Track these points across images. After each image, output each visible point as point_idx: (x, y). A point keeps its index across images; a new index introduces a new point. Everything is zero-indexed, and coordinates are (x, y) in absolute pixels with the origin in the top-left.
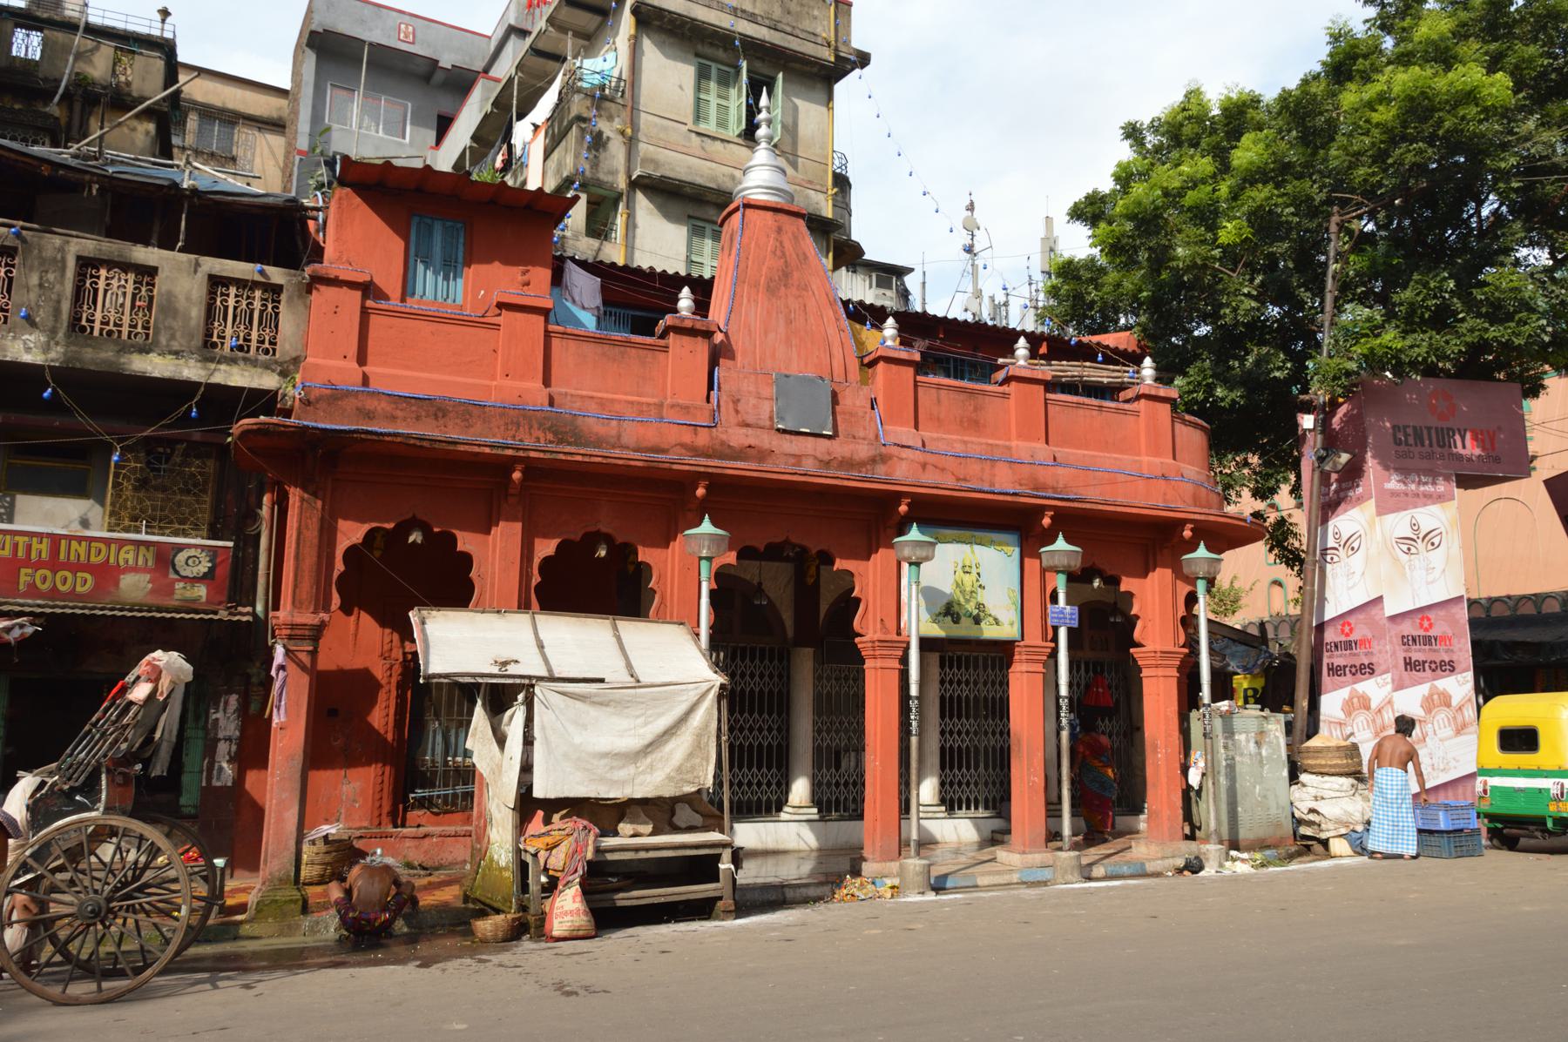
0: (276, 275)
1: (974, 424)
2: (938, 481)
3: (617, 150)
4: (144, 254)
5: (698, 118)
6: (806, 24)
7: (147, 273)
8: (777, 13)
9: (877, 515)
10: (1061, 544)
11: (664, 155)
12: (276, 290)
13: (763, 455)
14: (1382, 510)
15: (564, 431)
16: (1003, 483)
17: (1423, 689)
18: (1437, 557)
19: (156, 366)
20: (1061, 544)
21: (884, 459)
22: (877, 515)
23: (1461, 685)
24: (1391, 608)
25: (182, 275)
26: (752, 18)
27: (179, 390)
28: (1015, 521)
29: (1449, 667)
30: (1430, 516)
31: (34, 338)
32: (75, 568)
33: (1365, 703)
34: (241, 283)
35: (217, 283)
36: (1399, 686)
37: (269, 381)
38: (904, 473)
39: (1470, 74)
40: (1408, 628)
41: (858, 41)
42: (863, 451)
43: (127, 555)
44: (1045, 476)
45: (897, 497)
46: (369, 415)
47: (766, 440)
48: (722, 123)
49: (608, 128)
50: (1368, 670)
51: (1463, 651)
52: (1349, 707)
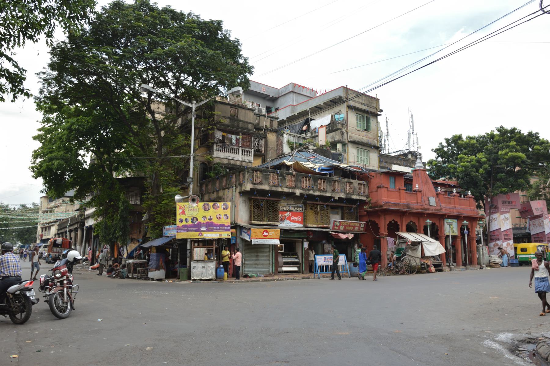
0: (365, 183)
1: (450, 203)
2: (448, 213)
3: (345, 134)
4: (352, 181)
5: (357, 126)
6: (373, 105)
7: (352, 183)
8: (368, 103)
9: (442, 217)
10: (465, 222)
11: (353, 135)
12: (364, 185)
13: (428, 209)
14: (501, 214)
15: (408, 207)
16: (455, 213)
17: (506, 243)
18: (508, 222)
19: (354, 197)
20: (465, 222)
21: (441, 209)
22: (442, 217)
23: (511, 242)
24: (502, 230)
25: (356, 183)
26: (364, 104)
27: (356, 200)
28: (458, 218)
29: (510, 239)
30: (507, 215)
31: (343, 194)
32: (351, 226)
33: (497, 245)
34: (361, 184)
35: (359, 184)
36: (503, 242)
37: (365, 199)
38: (443, 212)
39: (520, 154)
40: (504, 233)
41: (381, 108)
42: (439, 208)
43: (356, 225)
44: (461, 211)
45: (445, 215)
46: (389, 206)
47: (429, 207)
48: (360, 128)
49: (344, 130)
50: (498, 240)
51: (512, 237)
52: (494, 245)
